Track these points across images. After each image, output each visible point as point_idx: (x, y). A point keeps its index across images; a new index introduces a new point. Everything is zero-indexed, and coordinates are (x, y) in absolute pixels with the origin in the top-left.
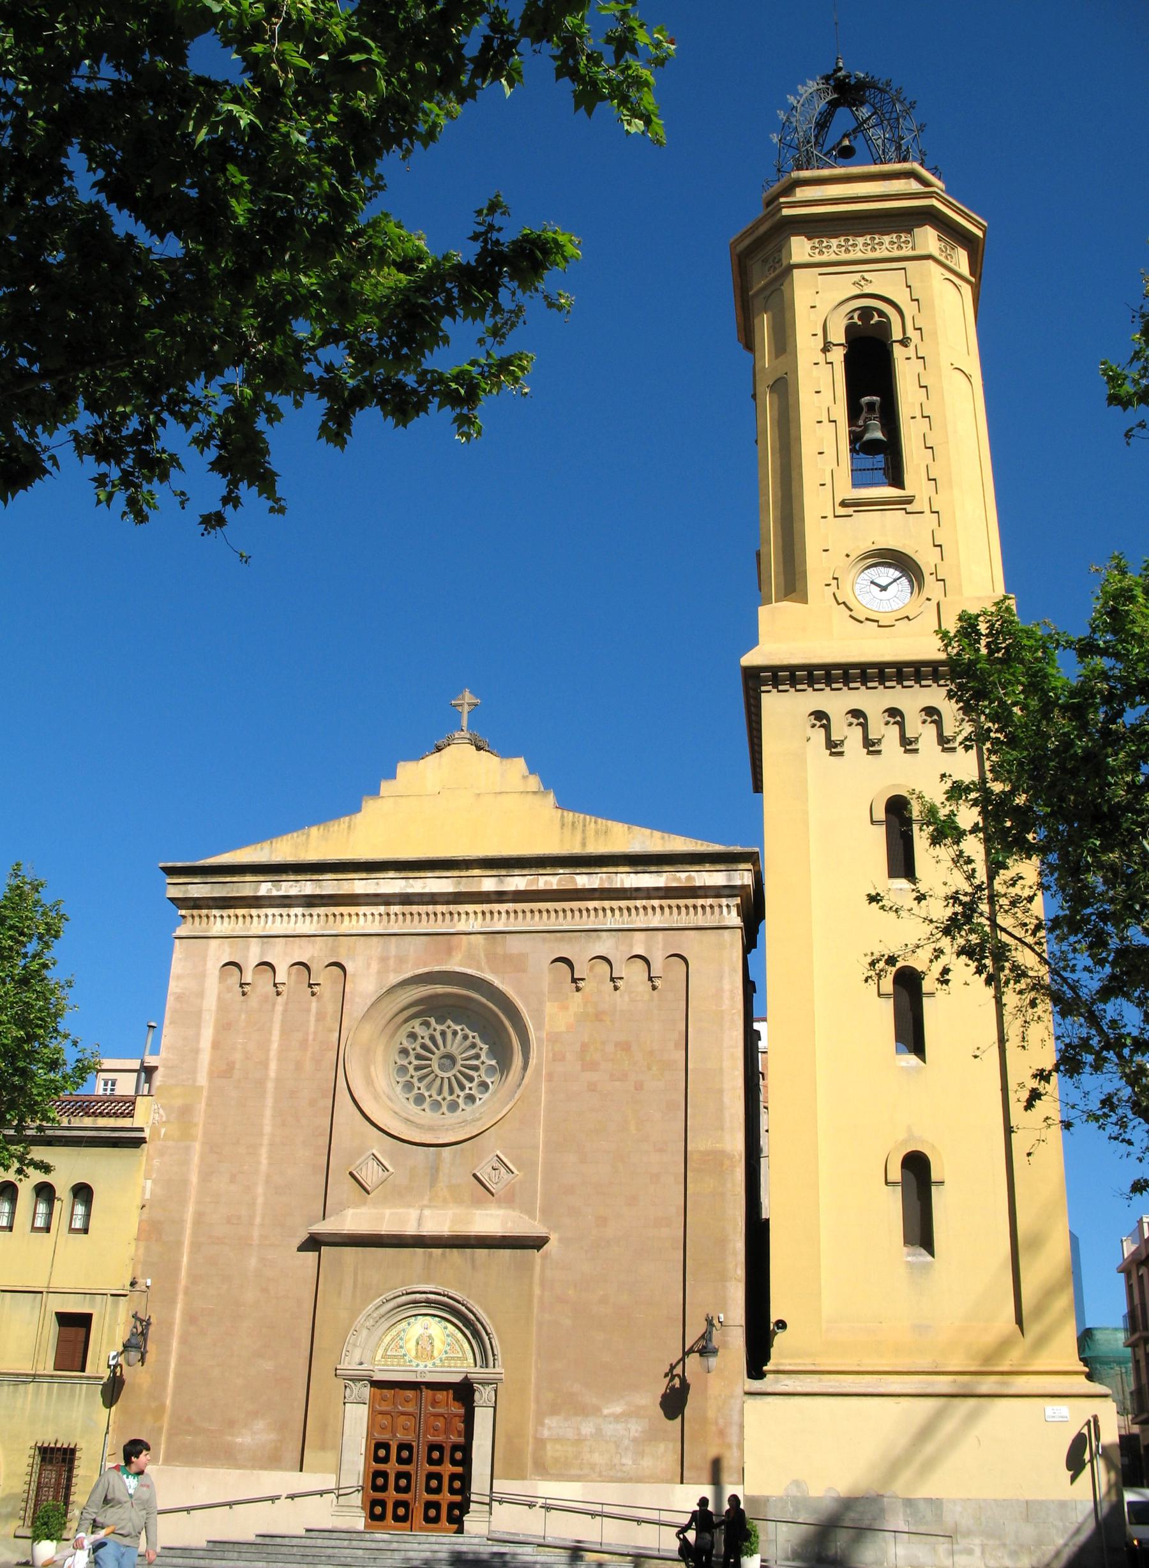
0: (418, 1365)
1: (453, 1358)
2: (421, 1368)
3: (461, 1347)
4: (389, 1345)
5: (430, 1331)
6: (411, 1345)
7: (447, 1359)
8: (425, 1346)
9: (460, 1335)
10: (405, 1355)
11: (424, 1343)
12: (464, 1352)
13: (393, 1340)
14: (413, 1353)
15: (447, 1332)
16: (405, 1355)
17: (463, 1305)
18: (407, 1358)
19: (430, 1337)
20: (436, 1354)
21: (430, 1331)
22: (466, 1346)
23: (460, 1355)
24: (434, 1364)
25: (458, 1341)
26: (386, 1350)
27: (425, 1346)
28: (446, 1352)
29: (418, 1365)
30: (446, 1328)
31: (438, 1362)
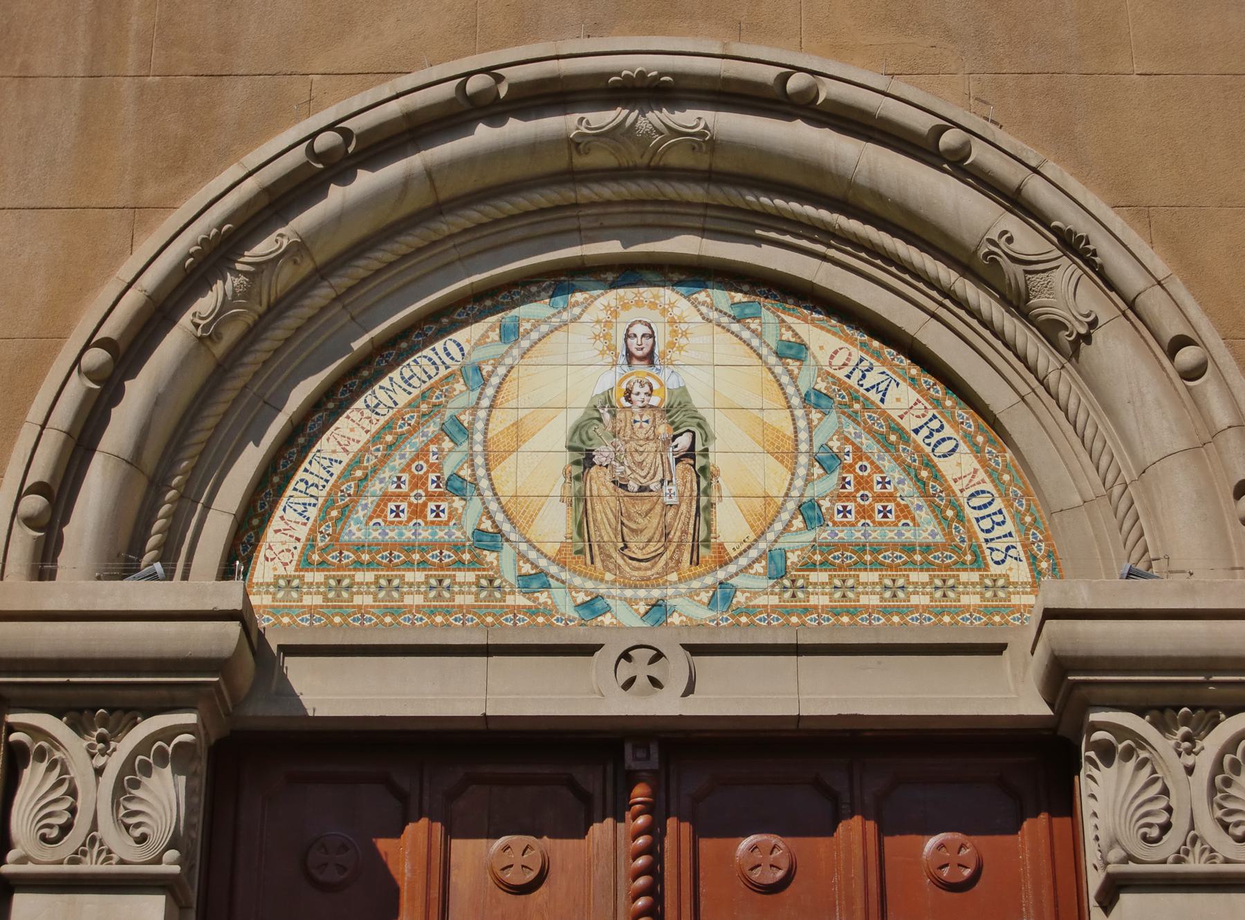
0: (592, 606)
1: (866, 555)
2: (625, 616)
3: (926, 476)
4: (359, 472)
5: (668, 379)
6: (534, 474)
7: (824, 557)
8: (645, 468)
9: (905, 398)
10: (489, 539)
11: (644, 454)
12: (946, 507)
13: (388, 439)
14: (553, 525)
15: (808, 379)
16: (489, 539)
17: (957, 164)
18: (505, 563)
19: (677, 411)
20: (730, 524)
21: (668, 379)
22: (960, 467)
23: (926, 529)
24: (723, 594)
25: (892, 436)
26: (337, 509)
27: (645, 468)
28: (810, 512)
29: (592, 606)
30: (794, 351)
31: (754, 588)
